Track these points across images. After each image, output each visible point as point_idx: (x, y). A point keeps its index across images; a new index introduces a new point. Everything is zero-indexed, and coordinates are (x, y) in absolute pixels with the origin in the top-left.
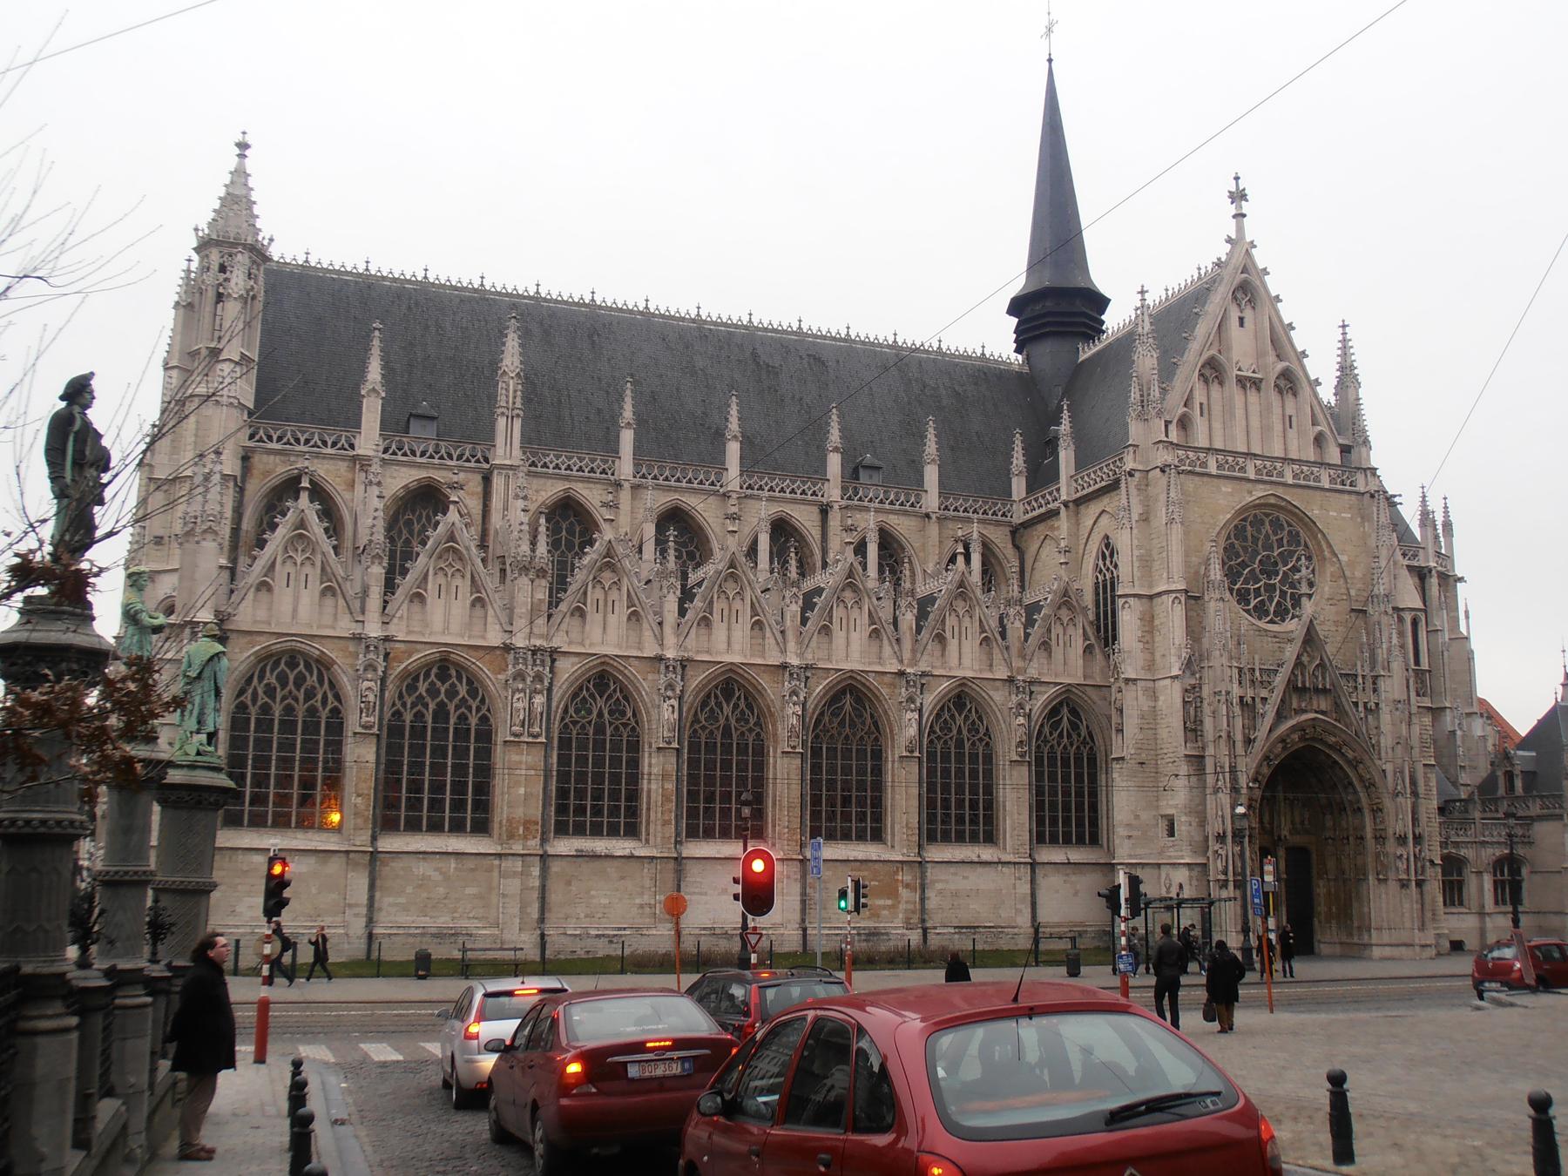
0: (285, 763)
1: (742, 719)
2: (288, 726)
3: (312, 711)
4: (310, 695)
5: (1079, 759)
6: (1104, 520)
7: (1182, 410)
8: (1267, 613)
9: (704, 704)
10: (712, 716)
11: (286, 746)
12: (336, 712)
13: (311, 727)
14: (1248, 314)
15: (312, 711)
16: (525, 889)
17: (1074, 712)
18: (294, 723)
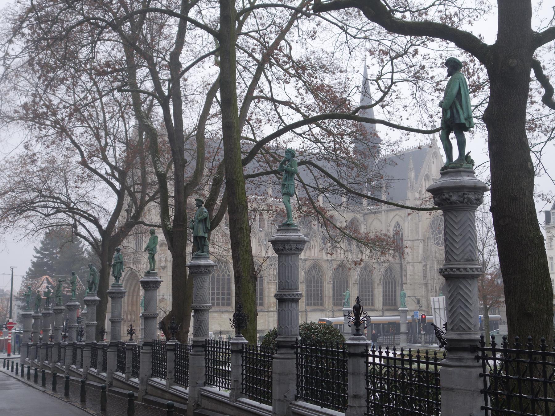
0: (218, 289)
1: (317, 274)
2: (218, 279)
3: (223, 275)
4: (223, 271)
5: (392, 283)
6: (397, 217)
7: (420, 189)
8: (439, 244)
9: (309, 270)
10: (311, 274)
11: (218, 284)
12: (229, 275)
13: (223, 279)
14: (435, 160)
15: (223, 275)
16: (274, 320)
17: (391, 270)
18: (220, 278)
